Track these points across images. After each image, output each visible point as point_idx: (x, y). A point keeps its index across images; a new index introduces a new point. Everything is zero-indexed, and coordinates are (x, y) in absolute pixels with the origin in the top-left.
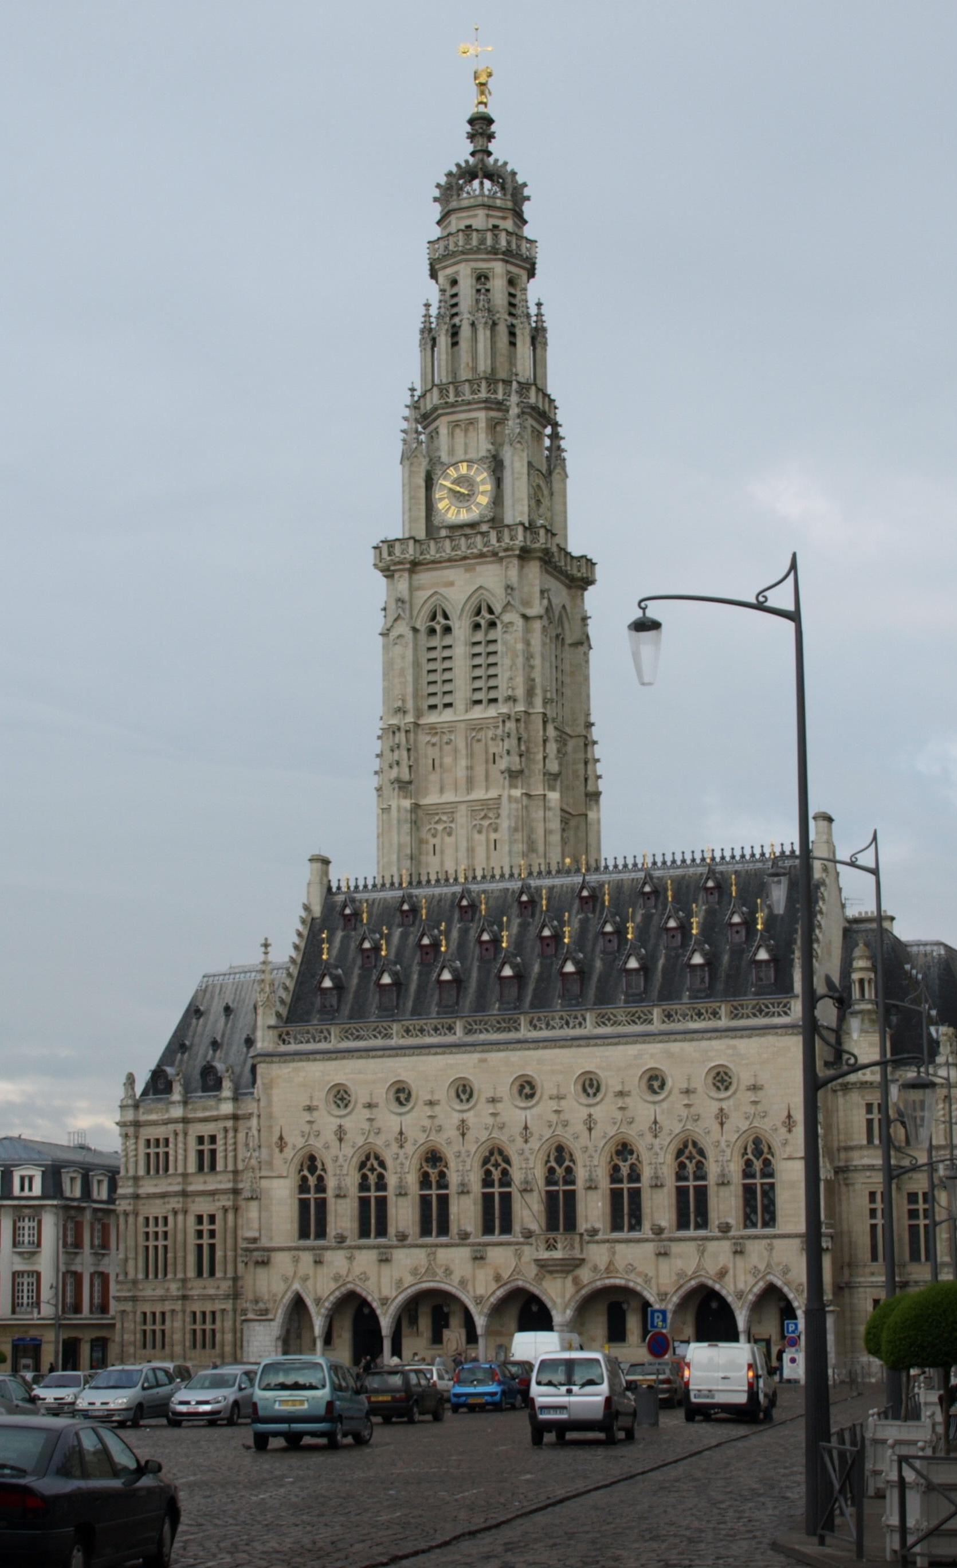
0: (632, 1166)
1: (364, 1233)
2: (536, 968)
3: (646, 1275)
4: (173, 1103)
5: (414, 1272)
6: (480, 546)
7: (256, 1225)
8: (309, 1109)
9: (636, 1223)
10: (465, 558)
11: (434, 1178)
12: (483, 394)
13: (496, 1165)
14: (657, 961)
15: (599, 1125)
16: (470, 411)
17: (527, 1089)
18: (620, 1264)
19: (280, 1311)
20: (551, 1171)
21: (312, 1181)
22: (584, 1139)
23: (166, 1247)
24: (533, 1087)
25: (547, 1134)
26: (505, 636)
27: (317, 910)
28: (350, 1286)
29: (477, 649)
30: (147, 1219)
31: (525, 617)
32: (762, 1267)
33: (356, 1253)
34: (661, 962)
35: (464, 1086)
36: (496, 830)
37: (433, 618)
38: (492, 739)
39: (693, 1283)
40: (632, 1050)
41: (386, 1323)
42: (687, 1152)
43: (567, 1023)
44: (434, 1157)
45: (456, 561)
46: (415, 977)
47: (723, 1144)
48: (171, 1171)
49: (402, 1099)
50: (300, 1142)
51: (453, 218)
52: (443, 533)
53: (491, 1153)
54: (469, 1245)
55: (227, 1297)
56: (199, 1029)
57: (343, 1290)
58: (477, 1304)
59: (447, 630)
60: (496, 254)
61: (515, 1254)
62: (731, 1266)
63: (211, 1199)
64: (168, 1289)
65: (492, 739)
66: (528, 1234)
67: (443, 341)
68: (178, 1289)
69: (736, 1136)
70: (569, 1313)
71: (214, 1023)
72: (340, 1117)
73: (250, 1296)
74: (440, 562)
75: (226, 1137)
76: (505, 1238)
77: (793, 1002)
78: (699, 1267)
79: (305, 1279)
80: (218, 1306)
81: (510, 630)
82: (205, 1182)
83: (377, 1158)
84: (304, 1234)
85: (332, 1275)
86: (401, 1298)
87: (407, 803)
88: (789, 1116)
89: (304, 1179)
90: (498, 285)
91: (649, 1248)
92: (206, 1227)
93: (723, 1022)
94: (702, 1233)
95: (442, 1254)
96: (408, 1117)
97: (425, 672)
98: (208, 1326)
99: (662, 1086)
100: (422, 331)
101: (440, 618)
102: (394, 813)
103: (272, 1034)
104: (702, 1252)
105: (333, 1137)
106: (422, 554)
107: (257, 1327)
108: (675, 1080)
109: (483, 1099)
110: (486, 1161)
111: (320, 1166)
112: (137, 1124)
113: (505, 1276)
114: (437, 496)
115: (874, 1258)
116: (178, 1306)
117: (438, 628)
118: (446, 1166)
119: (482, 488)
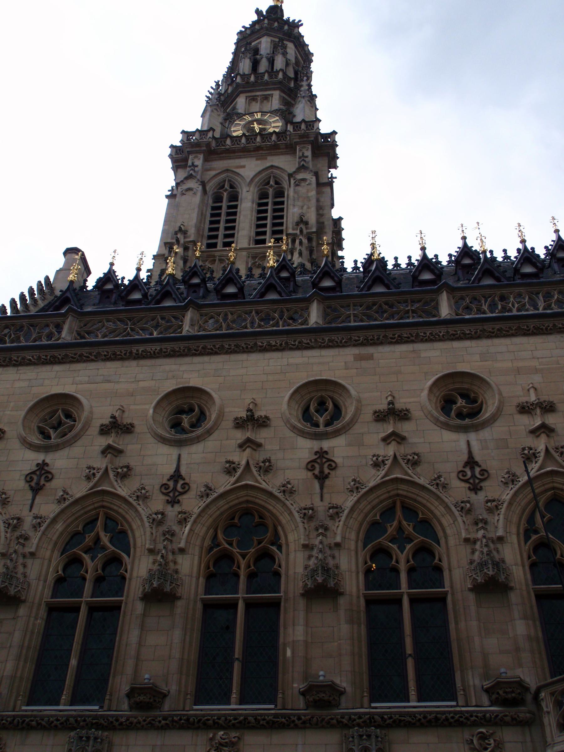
10: (258, 148)
16: (266, 90)
26: (297, 188)
45: (250, 151)
59: (234, 197)
81: (303, 184)
97: (207, 222)
101: (227, 186)
105: (22, 484)
114: (232, 129)
118: (276, 541)
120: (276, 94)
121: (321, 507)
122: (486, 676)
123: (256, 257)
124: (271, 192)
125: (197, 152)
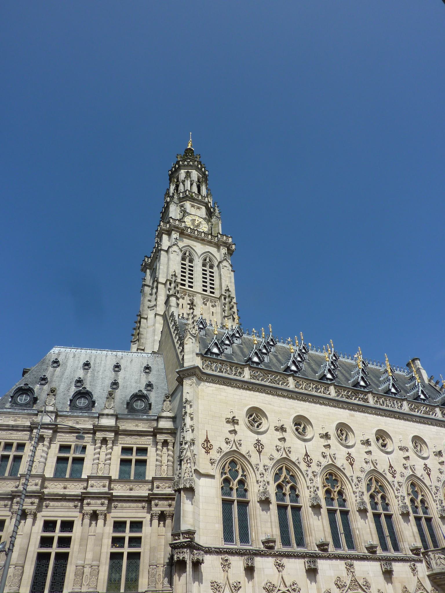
4: (47, 412)
11: (336, 496)
16: (199, 204)
33: (285, 561)
45: (198, 239)
54: (379, 559)
59: (191, 261)
65: (213, 306)
72: (259, 433)
74: (192, 237)
81: (225, 268)
82: (65, 488)
84: (228, 536)
85: (263, 585)
89: (226, 481)
111: (240, 473)
119: (204, 226)
120: (204, 208)
122: (409, 545)
123: (205, 299)
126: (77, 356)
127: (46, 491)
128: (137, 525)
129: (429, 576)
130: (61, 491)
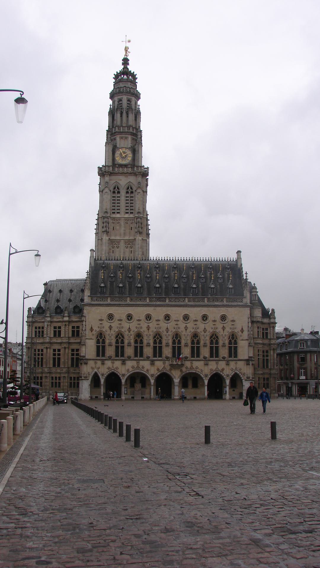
0: (198, 340)
1: (117, 356)
2: (164, 285)
3: (202, 370)
5: (133, 367)
6: (130, 170)
7: (84, 352)
8: (101, 320)
9: (198, 356)
12: (131, 131)
13: (158, 338)
14: (199, 286)
15: (189, 329)
16: (126, 135)
17: (167, 317)
18: (194, 367)
19: (90, 377)
20: (174, 341)
21: (101, 340)
22: (184, 333)
23: (42, 358)
24: (169, 317)
25: (174, 330)
26: (138, 196)
27: (93, 264)
28: (112, 371)
29: (127, 199)
30: (35, 350)
31: (143, 191)
32: (234, 369)
34: (200, 286)
35: (148, 316)
36: (131, 248)
37: (115, 188)
38: (131, 223)
39: (215, 372)
40: (199, 309)
41: (123, 381)
42: (213, 337)
43: (180, 301)
44: (139, 335)
46: (127, 285)
47: (224, 335)
48: (45, 336)
49: (129, 319)
50: (98, 330)
51: (121, 84)
52: (117, 166)
53: (156, 335)
55: (66, 373)
56: (51, 296)
57: (110, 372)
58: (152, 376)
59: (119, 192)
60: (133, 95)
61: (163, 363)
62: (225, 368)
63: (59, 344)
64: (44, 370)
65: (131, 223)
66: (167, 358)
67: (118, 116)
68: (48, 370)
69: (228, 333)
70: (179, 379)
71: (55, 294)
73: (83, 373)
74: (118, 174)
75: (65, 327)
76: (160, 358)
77: (244, 299)
78: (217, 368)
79: (99, 368)
80: (62, 375)
81: (139, 194)
82: (57, 340)
83: (121, 335)
84: (98, 355)
86: (128, 374)
87: (107, 238)
88: (242, 329)
89: (98, 340)
90: (133, 103)
91: (202, 363)
92: (57, 353)
93: (225, 303)
94: (217, 359)
95: (142, 363)
96: (131, 324)
98: (58, 381)
99: (206, 319)
100: (109, 113)
101: (116, 188)
102: (104, 241)
103: (90, 298)
104: (217, 364)
106: (113, 171)
107: (85, 382)
108: (211, 317)
109: (154, 320)
110: (155, 337)
111: (103, 336)
112: (33, 322)
113: (161, 369)
115: (258, 367)
116: (48, 375)
117: (116, 192)
118: (143, 338)
120: (130, 137)
121: (148, 334)
124: (130, 192)
125: (107, 174)
126: (57, 285)
127: (52, 341)
128: (77, 350)
129: (170, 365)
130: (56, 341)
